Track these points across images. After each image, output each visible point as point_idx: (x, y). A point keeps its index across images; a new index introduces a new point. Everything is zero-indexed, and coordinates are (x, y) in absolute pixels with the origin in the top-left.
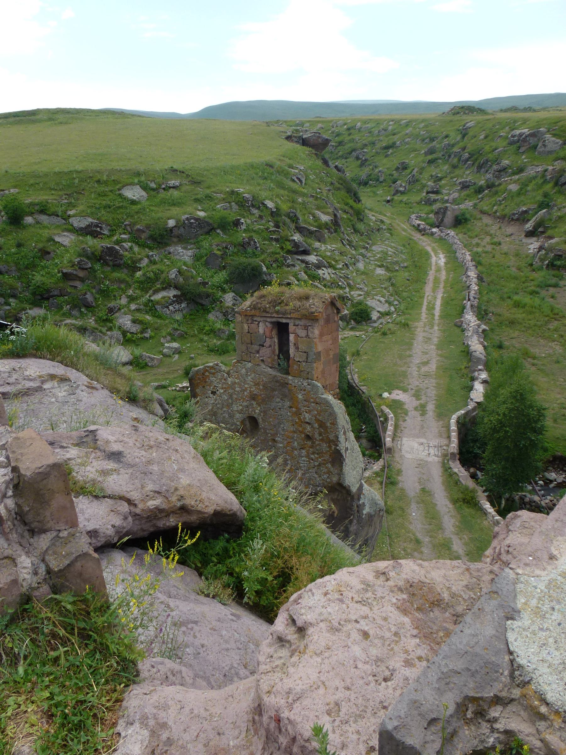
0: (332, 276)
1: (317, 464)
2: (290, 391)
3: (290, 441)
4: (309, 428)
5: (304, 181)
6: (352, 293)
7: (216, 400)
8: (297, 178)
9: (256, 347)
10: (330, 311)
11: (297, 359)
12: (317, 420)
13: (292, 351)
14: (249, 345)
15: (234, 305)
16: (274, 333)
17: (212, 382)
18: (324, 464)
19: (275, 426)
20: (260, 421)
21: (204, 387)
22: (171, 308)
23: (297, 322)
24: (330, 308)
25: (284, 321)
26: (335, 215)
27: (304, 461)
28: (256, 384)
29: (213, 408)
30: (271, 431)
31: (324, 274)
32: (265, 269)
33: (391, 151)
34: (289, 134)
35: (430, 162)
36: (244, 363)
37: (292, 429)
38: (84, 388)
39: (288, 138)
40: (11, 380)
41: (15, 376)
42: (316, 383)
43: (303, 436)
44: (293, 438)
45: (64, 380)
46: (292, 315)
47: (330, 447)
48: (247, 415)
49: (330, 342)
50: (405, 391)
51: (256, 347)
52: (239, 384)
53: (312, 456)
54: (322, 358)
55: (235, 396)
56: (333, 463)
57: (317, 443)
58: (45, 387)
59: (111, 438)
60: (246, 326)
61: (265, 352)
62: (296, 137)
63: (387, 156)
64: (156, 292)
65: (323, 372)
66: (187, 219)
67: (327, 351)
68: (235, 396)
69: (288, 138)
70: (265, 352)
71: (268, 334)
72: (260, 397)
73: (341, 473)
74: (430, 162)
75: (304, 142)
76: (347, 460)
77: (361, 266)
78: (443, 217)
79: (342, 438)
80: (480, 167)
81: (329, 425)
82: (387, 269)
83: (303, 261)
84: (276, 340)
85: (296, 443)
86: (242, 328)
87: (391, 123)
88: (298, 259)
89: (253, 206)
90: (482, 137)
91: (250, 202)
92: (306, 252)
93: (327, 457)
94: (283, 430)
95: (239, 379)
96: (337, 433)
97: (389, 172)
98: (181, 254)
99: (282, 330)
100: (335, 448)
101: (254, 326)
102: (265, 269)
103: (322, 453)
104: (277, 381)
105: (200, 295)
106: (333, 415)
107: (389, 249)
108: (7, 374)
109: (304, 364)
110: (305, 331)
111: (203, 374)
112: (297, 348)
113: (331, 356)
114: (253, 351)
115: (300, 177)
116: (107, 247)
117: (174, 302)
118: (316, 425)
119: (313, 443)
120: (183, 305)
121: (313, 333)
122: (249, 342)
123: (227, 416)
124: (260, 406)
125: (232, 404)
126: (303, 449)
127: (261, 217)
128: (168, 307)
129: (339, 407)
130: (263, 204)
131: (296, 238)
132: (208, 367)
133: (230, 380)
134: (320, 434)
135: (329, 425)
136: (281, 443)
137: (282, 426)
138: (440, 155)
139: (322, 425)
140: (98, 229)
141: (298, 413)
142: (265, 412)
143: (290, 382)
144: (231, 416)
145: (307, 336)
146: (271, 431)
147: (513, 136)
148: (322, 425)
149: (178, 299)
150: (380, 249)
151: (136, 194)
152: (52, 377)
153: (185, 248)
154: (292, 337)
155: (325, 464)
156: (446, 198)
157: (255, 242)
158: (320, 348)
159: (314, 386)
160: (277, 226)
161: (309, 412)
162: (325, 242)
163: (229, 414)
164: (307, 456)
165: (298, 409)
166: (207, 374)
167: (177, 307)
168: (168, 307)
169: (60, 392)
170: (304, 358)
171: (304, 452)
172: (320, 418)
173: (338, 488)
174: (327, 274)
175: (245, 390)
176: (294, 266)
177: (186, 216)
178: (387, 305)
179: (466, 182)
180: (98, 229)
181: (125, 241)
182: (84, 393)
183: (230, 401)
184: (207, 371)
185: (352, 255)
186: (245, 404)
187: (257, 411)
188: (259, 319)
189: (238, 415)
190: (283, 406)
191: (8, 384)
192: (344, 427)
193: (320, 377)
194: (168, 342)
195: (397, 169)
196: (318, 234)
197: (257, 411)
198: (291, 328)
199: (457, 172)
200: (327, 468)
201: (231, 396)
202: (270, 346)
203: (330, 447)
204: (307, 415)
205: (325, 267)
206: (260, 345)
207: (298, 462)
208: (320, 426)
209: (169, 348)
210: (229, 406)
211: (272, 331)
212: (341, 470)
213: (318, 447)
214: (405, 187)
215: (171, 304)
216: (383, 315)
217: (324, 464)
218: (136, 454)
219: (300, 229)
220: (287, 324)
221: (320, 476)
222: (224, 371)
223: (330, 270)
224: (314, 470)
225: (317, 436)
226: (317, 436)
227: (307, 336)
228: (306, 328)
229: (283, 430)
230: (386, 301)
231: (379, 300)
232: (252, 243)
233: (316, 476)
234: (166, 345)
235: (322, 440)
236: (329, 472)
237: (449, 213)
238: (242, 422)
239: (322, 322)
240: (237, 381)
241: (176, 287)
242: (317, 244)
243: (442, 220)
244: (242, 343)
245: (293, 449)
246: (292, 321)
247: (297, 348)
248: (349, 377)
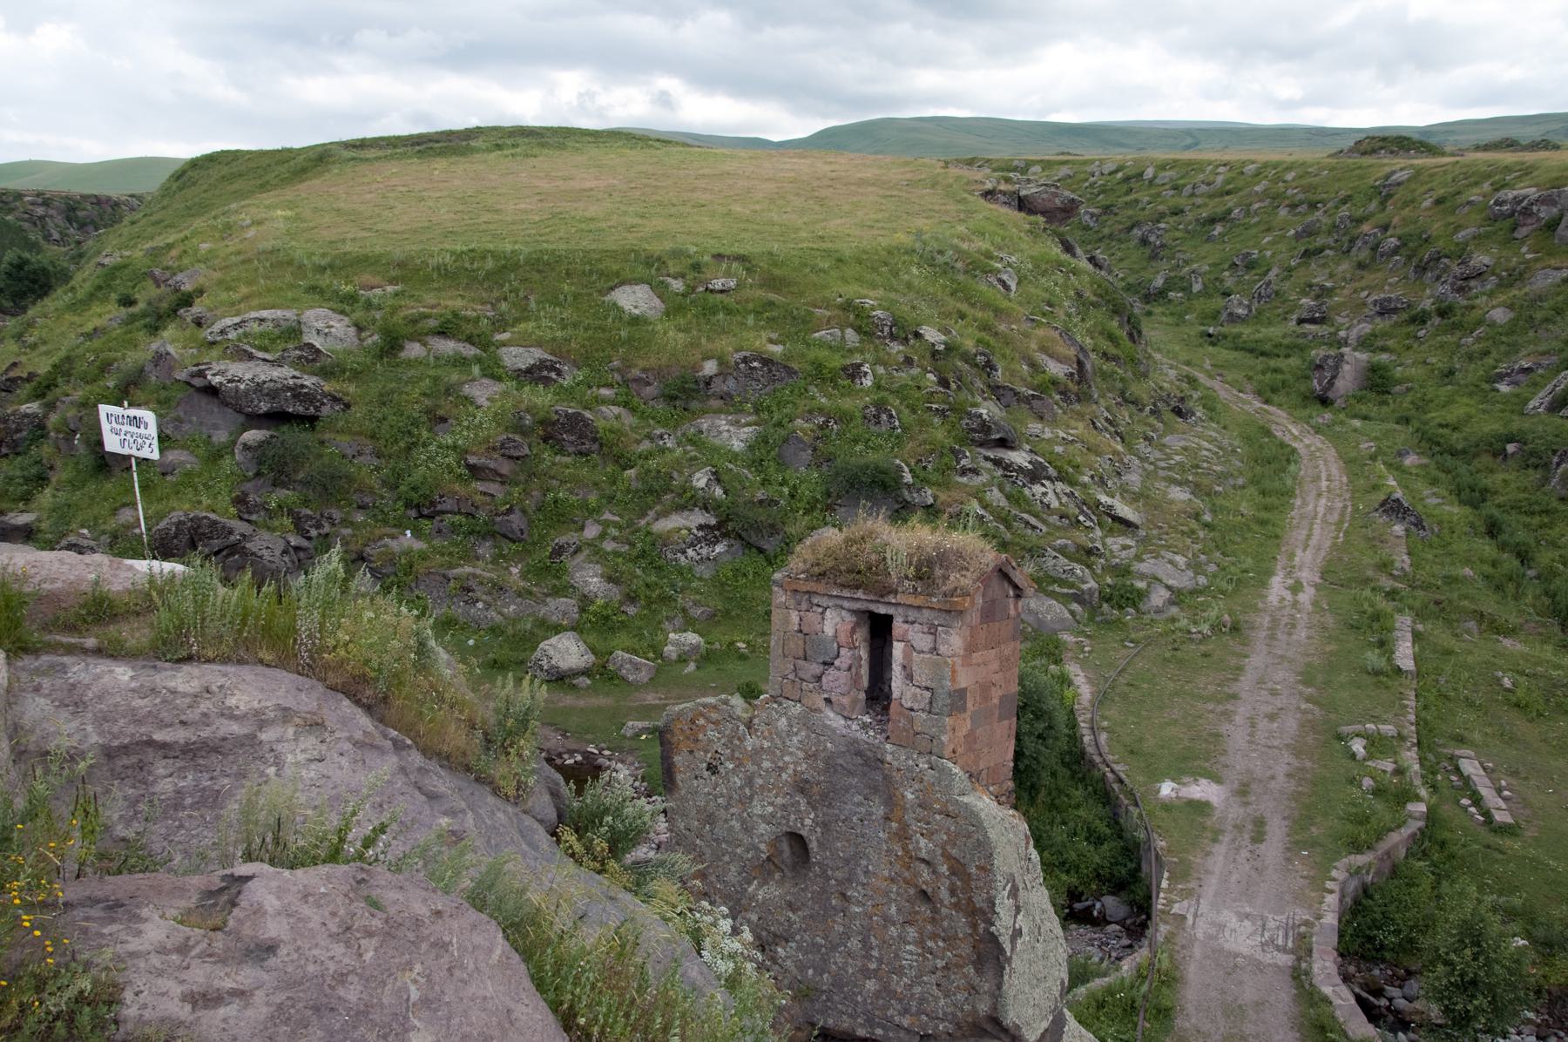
0: (1065, 499)
1: (940, 963)
2: (886, 777)
3: (881, 900)
4: (926, 874)
5: (1013, 288)
6: (1109, 541)
7: (716, 785)
9: (816, 669)
10: (998, 589)
11: (909, 705)
12: (947, 856)
13: (897, 683)
14: (801, 662)
16: (862, 635)
17: (710, 741)
18: (956, 965)
19: (847, 861)
20: (813, 845)
21: (691, 752)
22: (690, 552)
23: (912, 615)
24: (995, 581)
25: (882, 610)
26: (1080, 363)
27: (911, 953)
28: (808, 757)
29: (707, 803)
30: (839, 874)
31: (1045, 494)
32: (908, 478)
33: (1218, 229)
34: (989, 186)
35: (1307, 254)
36: (787, 703)
37: (886, 873)
38: (347, 746)
39: (989, 194)
40: (191, 715)
41: (205, 706)
42: (950, 765)
43: (912, 891)
44: (887, 894)
45: (315, 725)
46: (900, 598)
47: (974, 926)
48: (785, 829)
49: (995, 666)
50: (1217, 779)
51: (816, 669)
52: (769, 751)
53: (930, 944)
54: (969, 705)
55: (760, 781)
56: (979, 964)
57: (944, 911)
58: (263, 736)
59: (271, 903)
61: (836, 679)
62: (1004, 193)
63: (1209, 239)
64: (664, 514)
65: (970, 738)
66: (745, 360)
67: (985, 689)
68: (760, 781)
69: (989, 194)
70: (836, 679)
71: (843, 638)
72: (816, 789)
73: (997, 993)
75: (1023, 204)
76: (1016, 963)
77: (1134, 479)
78: (1334, 377)
79: (1004, 906)
80: (1422, 269)
81: (973, 870)
82: (1196, 489)
83: (997, 462)
84: (864, 654)
85: (894, 909)
86: (787, 621)
87: (1221, 169)
88: (987, 458)
89: (893, 337)
91: (886, 329)
92: (1003, 443)
93: (965, 949)
94: (867, 872)
95: (772, 740)
96: (993, 892)
98: (725, 435)
99: (879, 630)
100: (987, 931)
102: (908, 478)
103: (956, 937)
104: (859, 753)
105: (757, 527)
106: (984, 848)
107: (1206, 444)
108: (188, 700)
109: (924, 716)
110: (931, 637)
111: (693, 721)
112: (910, 677)
113: (996, 701)
114: (807, 676)
115: (1005, 277)
116: (567, 415)
118: (944, 869)
119: (935, 911)
120: (719, 548)
121: (946, 642)
122: (801, 653)
123: (736, 824)
124: (814, 808)
125: (751, 798)
126: (909, 923)
127: (908, 361)
128: (684, 552)
129: (1006, 831)
130: (917, 335)
131: (984, 411)
132: (705, 706)
133: (750, 743)
134: (953, 892)
135: (973, 870)
136: (859, 903)
137: (864, 862)
138: (1330, 241)
139: (958, 869)
140: (553, 375)
141: (903, 835)
142: (825, 825)
143: (889, 758)
144: (747, 830)
145: (934, 650)
146: (839, 874)
148: (958, 869)
149: (712, 534)
150: (1183, 443)
151: (641, 303)
152: (286, 714)
153: (737, 423)
154: (898, 649)
155: (962, 967)
156: (1342, 334)
157: (891, 416)
158: (964, 681)
159: (943, 771)
160: (944, 382)
161: (929, 835)
162: (1054, 422)
163: (743, 822)
164: (920, 943)
165: (904, 827)
166: (702, 721)
167: (704, 551)
168: (684, 552)
169: (293, 752)
170: (924, 704)
171: (912, 932)
172: (954, 852)
173: (989, 1027)
174: (1051, 496)
175: (782, 769)
176: (975, 472)
177: (744, 353)
178: (1190, 573)
180: (553, 375)
181: (604, 401)
182: (344, 761)
183: (747, 791)
184: (702, 715)
185: (1115, 452)
186: (779, 801)
187: (807, 825)
188: (824, 602)
189: (763, 828)
190: (871, 814)
191: (183, 723)
192: (1011, 878)
193: (960, 750)
194: (675, 631)
196: (1035, 403)
197: (808, 822)
198: (898, 626)
200: (965, 976)
201: (749, 781)
202: (850, 669)
203: (974, 926)
204: (923, 842)
205: (1049, 478)
206: (825, 663)
207: (897, 956)
208: (953, 872)
209: (677, 644)
210: (745, 801)
211: (853, 631)
212: (999, 986)
213: (945, 923)
214: (1249, 307)
215: (692, 545)
216: (1178, 597)
217: (956, 965)
218: (315, 952)
219: (997, 391)
220: (888, 619)
221: (946, 996)
222: (739, 718)
223: (1060, 486)
224: (933, 979)
225: (944, 894)
226: (944, 894)
227: (934, 650)
228: (932, 631)
229: (867, 872)
230: (1188, 565)
231: (1170, 562)
232: (884, 417)
233: (936, 992)
234: (672, 635)
235: (956, 906)
236: (973, 989)
237: (1346, 367)
238: (774, 843)
239: (974, 617)
240: (766, 744)
242: (1035, 427)
243: (1331, 383)
245: (888, 920)
246: (900, 610)
247: (910, 677)
248: (1086, 739)
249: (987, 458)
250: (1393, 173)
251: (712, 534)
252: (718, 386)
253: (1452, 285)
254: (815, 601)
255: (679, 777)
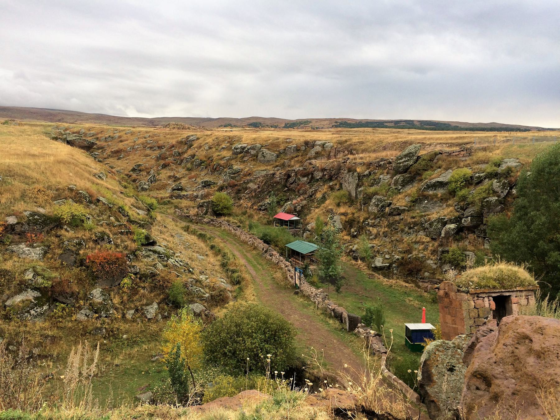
0: (181, 263)
8: (99, 176)
15: (104, 300)
22: (32, 312)
25: (507, 294)
60: (473, 304)
63: (119, 159)
74: (165, 166)
86: (469, 305)
87: (116, 132)
88: (150, 250)
90: (207, 148)
97: (126, 172)
101: (480, 302)
115: (101, 175)
117: (36, 305)
120: (45, 308)
128: (28, 312)
147: (237, 149)
149: (39, 302)
153: (32, 246)
168: (28, 312)
176: (149, 256)
179: (207, 181)
188: (484, 295)
195: (134, 170)
198: (514, 299)
199: (193, 174)
214: (148, 185)
215: (32, 308)
232: (106, 237)
241: (35, 289)
244: (470, 319)
249: (150, 250)
250: (189, 136)
251: (39, 302)
252: (18, 229)
253: (229, 176)
254: (480, 296)
255: (435, 378)
